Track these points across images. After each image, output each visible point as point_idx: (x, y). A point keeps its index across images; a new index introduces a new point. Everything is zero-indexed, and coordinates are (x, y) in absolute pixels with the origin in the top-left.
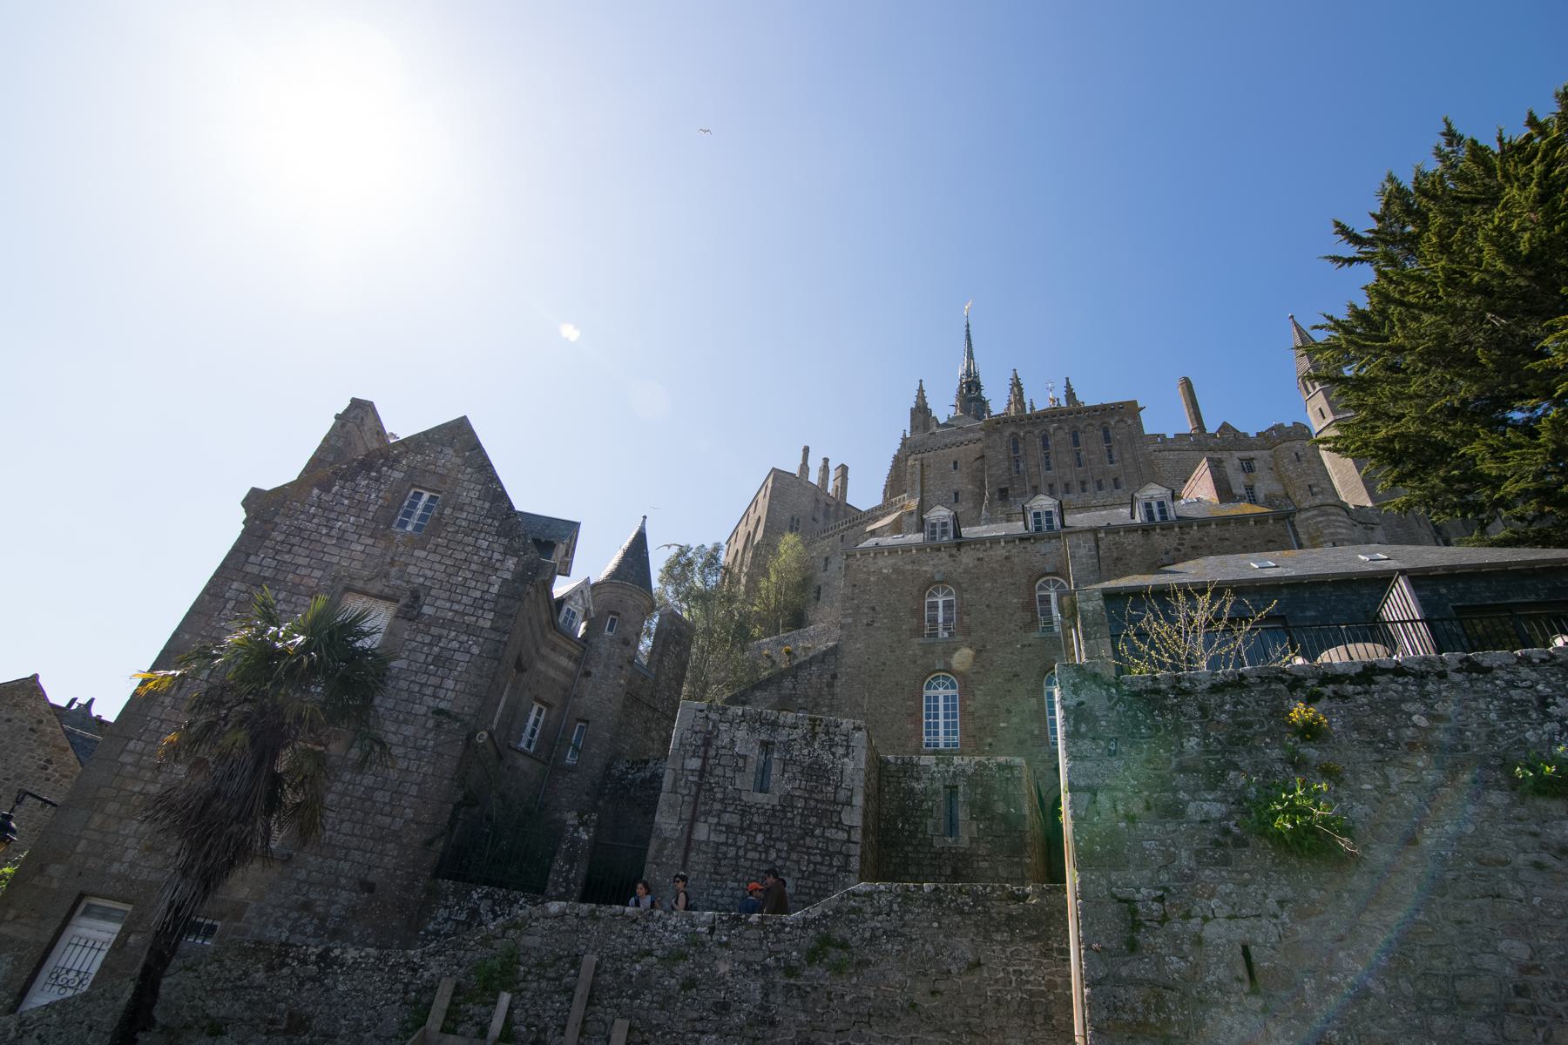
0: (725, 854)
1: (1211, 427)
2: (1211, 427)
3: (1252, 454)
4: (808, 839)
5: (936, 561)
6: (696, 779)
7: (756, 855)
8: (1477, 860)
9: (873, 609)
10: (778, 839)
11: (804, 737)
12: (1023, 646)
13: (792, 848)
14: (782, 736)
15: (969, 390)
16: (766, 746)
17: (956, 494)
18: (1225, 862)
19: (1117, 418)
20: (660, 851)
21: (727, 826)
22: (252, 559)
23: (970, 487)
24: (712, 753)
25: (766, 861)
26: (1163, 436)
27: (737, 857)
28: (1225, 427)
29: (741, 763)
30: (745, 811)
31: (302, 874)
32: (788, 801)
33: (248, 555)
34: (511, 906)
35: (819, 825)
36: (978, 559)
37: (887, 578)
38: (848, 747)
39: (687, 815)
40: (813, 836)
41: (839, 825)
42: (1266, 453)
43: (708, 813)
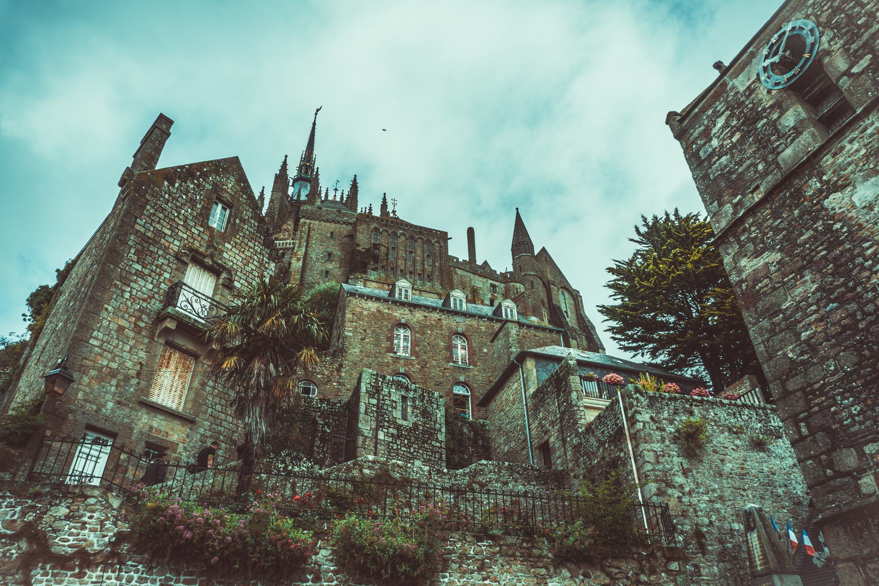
0: (392, 447)
1: (479, 262)
2: (479, 262)
3: (497, 283)
4: (426, 445)
5: (401, 311)
6: (375, 409)
7: (405, 449)
8: (723, 447)
9: (365, 330)
10: (413, 443)
11: (420, 396)
12: (445, 369)
13: (420, 448)
14: (411, 395)
15: (306, 172)
16: (404, 399)
17: (330, 254)
18: (675, 443)
19: (436, 240)
20: (364, 442)
21: (392, 434)
22: (138, 220)
23: (339, 253)
24: (381, 397)
25: (410, 452)
26: (457, 259)
27: (397, 449)
28: (486, 263)
29: (394, 404)
30: (399, 427)
31: (202, 431)
32: (415, 425)
33: (136, 218)
34: (300, 461)
35: (429, 438)
36: (425, 316)
37: (373, 314)
38: (438, 405)
39: (374, 426)
40: (427, 443)
41: (437, 440)
42: (503, 285)
43: (383, 427)
